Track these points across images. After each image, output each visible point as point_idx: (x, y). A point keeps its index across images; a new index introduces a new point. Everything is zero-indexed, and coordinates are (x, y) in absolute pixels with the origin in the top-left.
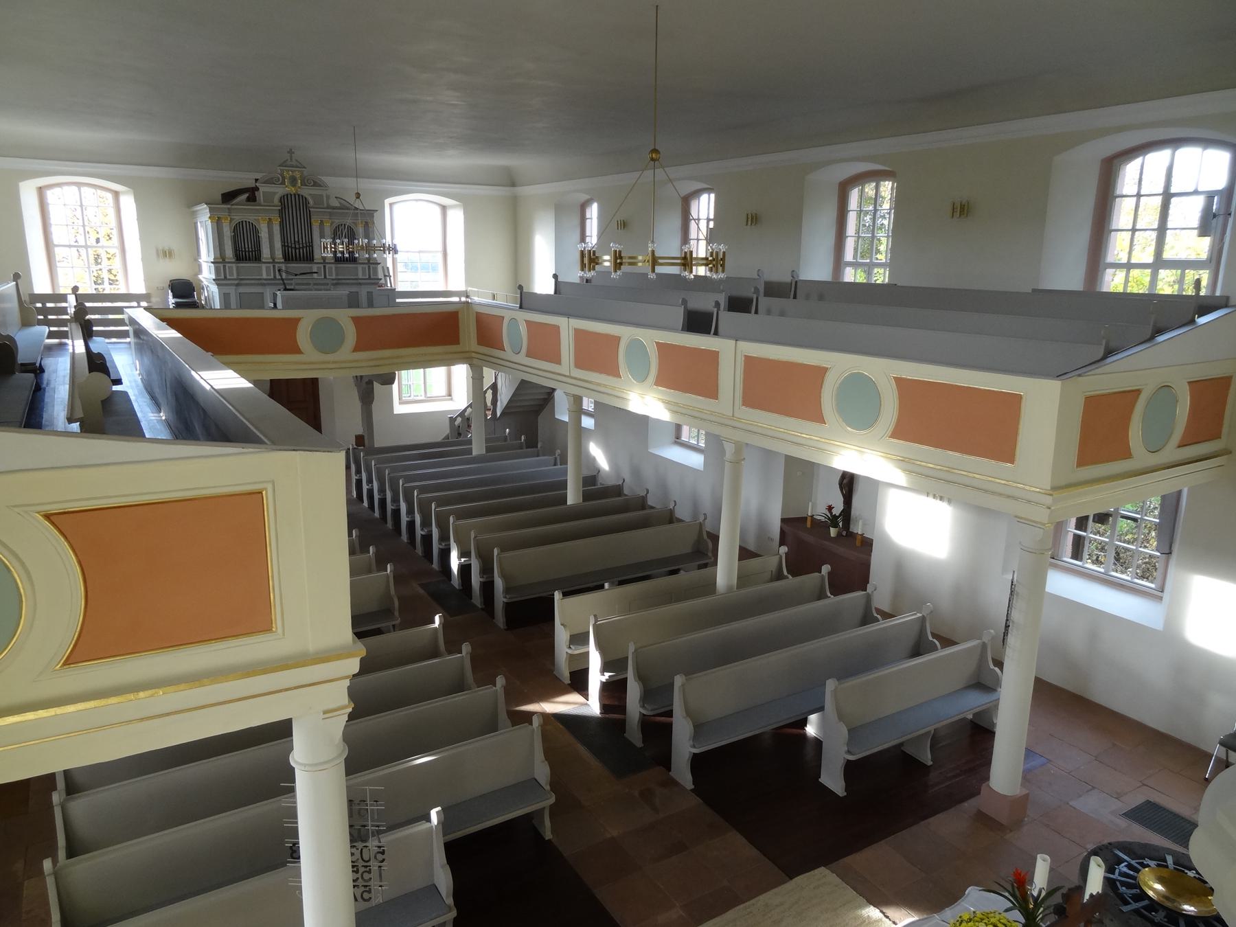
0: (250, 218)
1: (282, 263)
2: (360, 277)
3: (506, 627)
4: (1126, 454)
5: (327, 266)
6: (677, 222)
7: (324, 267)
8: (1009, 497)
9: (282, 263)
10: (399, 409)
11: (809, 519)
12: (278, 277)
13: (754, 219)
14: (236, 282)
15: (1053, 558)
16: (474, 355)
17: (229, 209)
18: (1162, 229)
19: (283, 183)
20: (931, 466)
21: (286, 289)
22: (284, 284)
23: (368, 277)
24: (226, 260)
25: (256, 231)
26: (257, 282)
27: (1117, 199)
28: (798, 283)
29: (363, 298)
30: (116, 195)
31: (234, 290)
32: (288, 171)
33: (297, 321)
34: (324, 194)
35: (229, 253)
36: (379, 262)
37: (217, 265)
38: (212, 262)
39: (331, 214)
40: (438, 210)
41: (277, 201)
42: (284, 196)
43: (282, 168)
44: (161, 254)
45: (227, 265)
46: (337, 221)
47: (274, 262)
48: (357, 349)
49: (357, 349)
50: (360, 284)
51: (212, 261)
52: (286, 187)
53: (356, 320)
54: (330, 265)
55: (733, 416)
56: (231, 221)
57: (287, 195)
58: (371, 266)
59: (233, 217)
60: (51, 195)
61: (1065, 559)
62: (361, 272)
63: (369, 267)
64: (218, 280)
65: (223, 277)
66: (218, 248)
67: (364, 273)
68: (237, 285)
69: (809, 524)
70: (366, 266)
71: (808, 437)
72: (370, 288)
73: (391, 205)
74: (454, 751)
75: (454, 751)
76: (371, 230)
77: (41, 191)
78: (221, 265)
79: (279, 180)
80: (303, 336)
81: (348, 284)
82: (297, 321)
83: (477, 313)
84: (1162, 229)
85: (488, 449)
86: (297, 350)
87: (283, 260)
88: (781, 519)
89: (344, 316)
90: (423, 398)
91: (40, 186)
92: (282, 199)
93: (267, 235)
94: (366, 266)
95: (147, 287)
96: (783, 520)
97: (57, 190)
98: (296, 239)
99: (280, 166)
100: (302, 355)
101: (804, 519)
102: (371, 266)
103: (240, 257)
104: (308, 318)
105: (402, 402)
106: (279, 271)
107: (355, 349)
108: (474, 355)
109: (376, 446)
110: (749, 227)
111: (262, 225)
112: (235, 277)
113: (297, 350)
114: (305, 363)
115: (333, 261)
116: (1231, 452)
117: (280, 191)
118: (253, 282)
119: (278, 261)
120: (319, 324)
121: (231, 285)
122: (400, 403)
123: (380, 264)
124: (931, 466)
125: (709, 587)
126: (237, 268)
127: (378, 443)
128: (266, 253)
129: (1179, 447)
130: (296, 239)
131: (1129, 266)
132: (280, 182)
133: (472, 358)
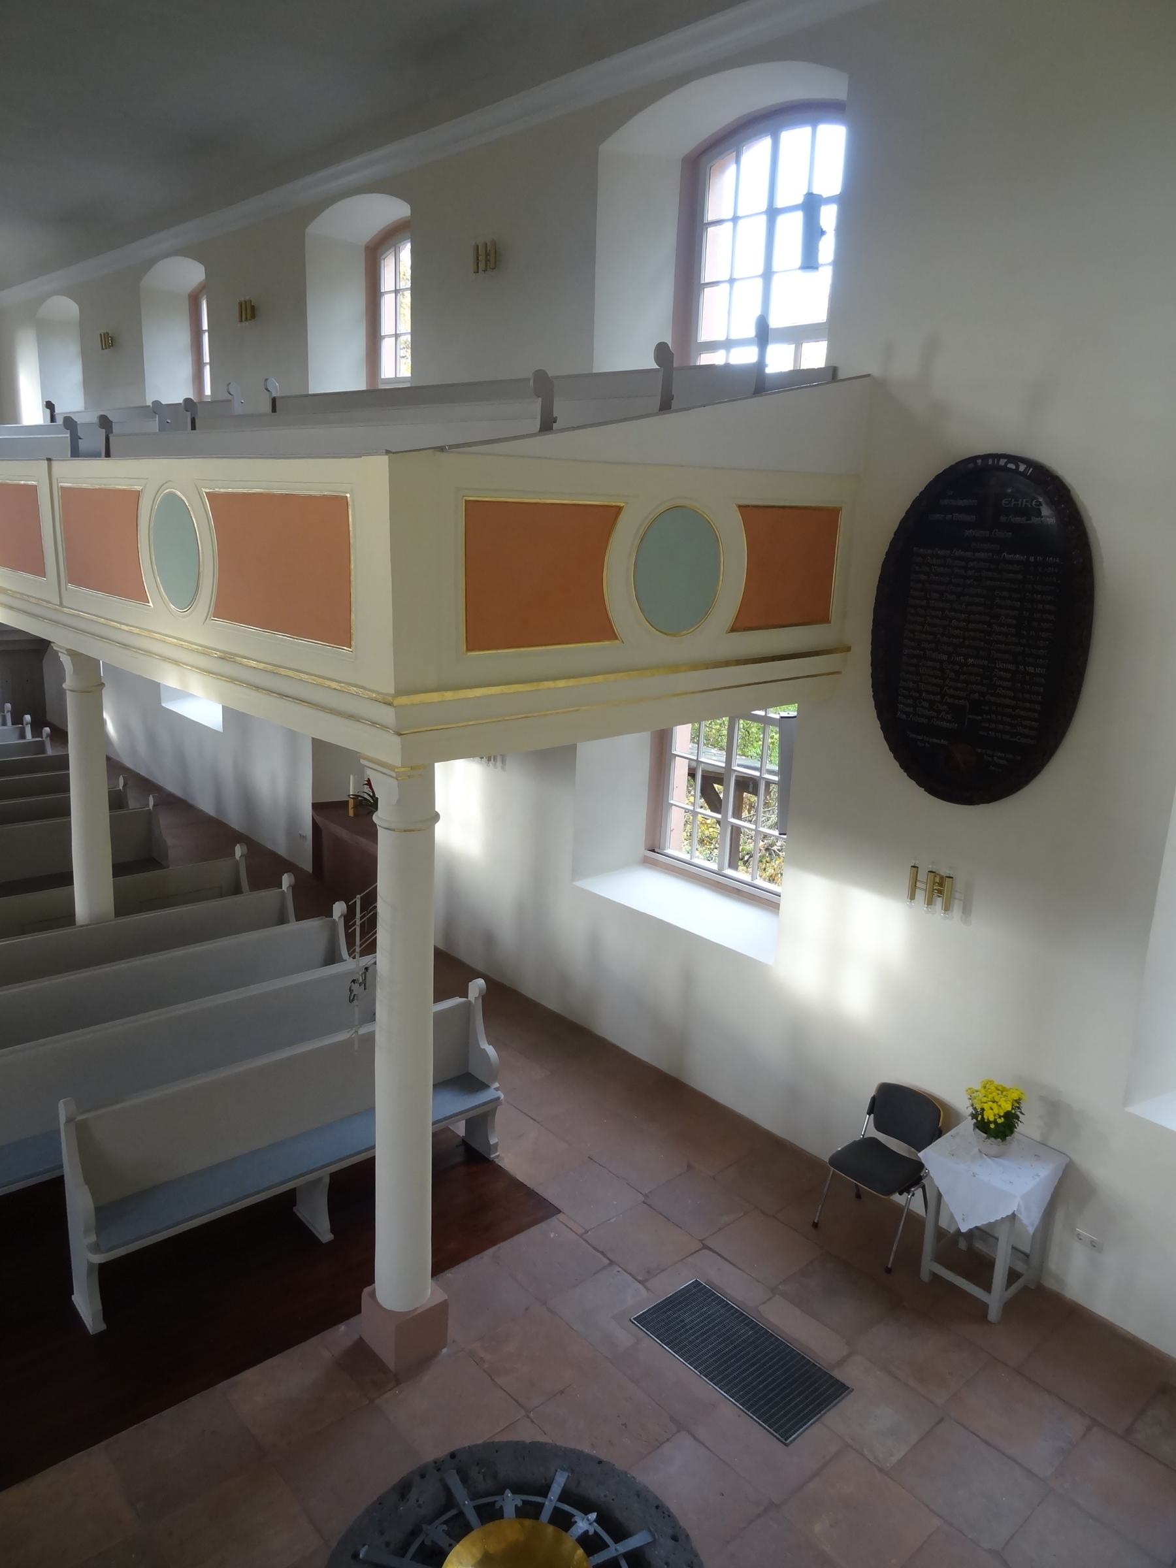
4: (604, 630)
6: (183, 338)
8: (351, 717)
11: (351, 803)
13: (249, 312)
15: (653, 851)
18: (768, 274)
20: (253, 664)
27: (711, 230)
28: (277, 400)
55: (61, 604)
61: (668, 851)
69: (351, 813)
71: (126, 628)
84: (768, 274)
88: (312, 804)
96: (316, 807)
101: (345, 804)
110: (243, 324)
116: (848, 649)
124: (253, 664)
125: (68, 917)
129: (733, 630)
131: (728, 344)
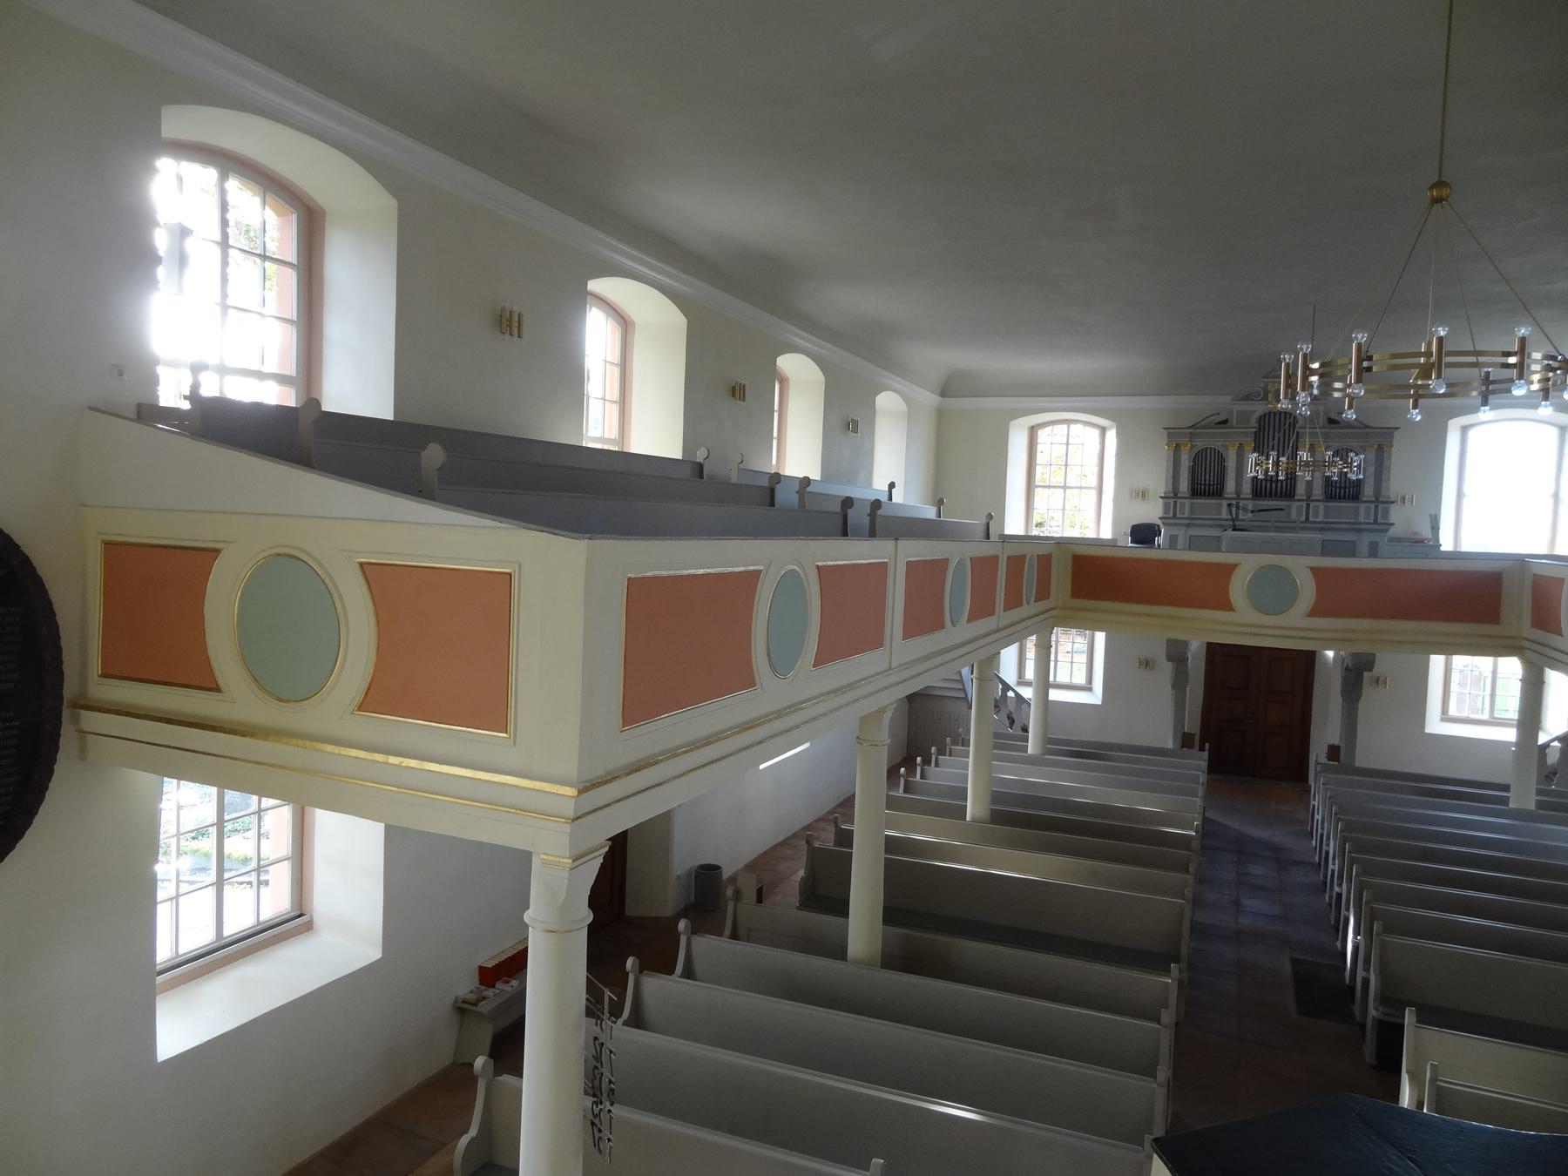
0: (1217, 444)
1: (1250, 499)
2: (1362, 519)
3: (1374, 1062)
5: (1312, 504)
7: (1308, 505)
9: (1250, 499)
10: (1435, 725)
12: (1224, 514)
14: (1188, 521)
16: (1525, 644)
17: (1191, 433)
19: (1265, 398)
21: (1235, 529)
22: (1235, 526)
23: (1372, 521)
24: (1179, 495)
25: (1221, 460)
26: (1216, 522)
29: (1364, 545)
30: (1103, 430)
31: (1183, 532)
33: (1230, 568)
35: (1184, 486)
36: (1392, 499)
38: (1161, 497)
40: (1554, 432)
41: (1255, 421)
43: (1266, 380)
44: (1137, 494)
45: (1179, 501)
47: (1238, 497)
48: (1314, 612)
49: (1314, 612)
50: (1360, 530)
51: (1163, 495)
52: (1269, 403)
53: (1317, 572)
54: (1318, 503)
57: (1270, 413)
58: (1380, 506)
59: (1195, 443)
60: (1043, 435)
62: (1363, 512)
63: (1376, 507)
64: (1167, 518)
65: (1171, 515)
67: (1367, 515)
68: (1188, 526)
70: (1372, 506)
72: (1374, 537)
73: (1465, 429)
74: (1009, 1125)
75: (1009, 1125)
76: (1385, 455)
77: (1033, 432)
78: (1172, 501)
79: (1260, 395)
80: (1237, 590)
81: (1338, 529)
82: (1230, 568)
83: (1534, 575)
85: (1540, 805)
86: (1228, 607)
87: (1251, 496)
89: (1300, 567)
90: (1486, 716)
91: (1031, 424)
92: (1261, 419)
93: (1234, 465)
94: (1372, 506)
95: (1114, 532)
97: (1048, 429)
99: (1264, 378)
100: (1233, 613)
102: (1380, 506)
103: (1196, 492)
104: (1247, 565)
105: (1446, 718)
106: (1229, 505)
107: (1313, 610)
108: (1525, 644)
109: (1357, 765)
112: (1186, 516)
113: (1228, 607)
114: (1240, 625)
115: (1321, 498)
117: (1259, 408)
118: (1207, 522)
119: (1229, 496)
120: (1262, 574)
121: (1180, 525)
122: (1443, 720)
123: (1393, 502)
126: (1192, 505)
127: (1361, 761)
128: (1230, 486)
133: (1523, 648)
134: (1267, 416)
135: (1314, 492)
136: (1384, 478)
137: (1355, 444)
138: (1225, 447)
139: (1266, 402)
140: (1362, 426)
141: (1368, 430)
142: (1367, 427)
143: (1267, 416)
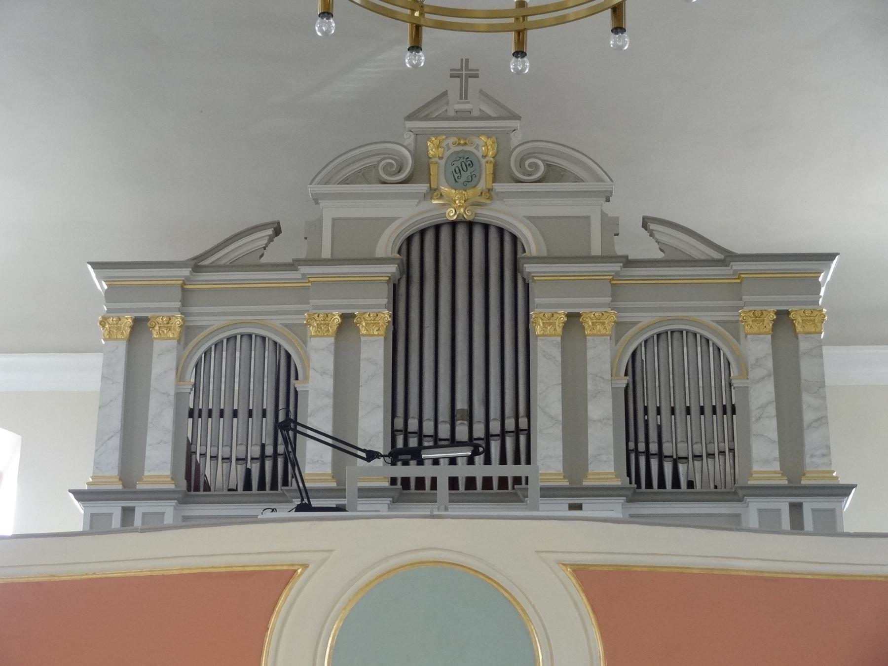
32: (448, 133)
34: (592, 210)
36: (842, 481)
37: (101, 508)
38: (81, 495)
39: (616, 290)
42: (422, 232)
46: (646, 319)
52: (433, 192)
56: (188, 332)
66: (115, 442)
93: (328, 384)
98: (461, 404)
99: (411, 117)
111: (314, 343)
123: (844, 490)
130: (461, 404)
132: (403, 176)
134: (429, 238)
135: (592, 468)
136: (808, 416)
137: (707, 318)
138: (300, 332)
139: (423, 188)
140: (717, 255)
141: (737, 266)
142: (728, 257)
143: (429, 238)
